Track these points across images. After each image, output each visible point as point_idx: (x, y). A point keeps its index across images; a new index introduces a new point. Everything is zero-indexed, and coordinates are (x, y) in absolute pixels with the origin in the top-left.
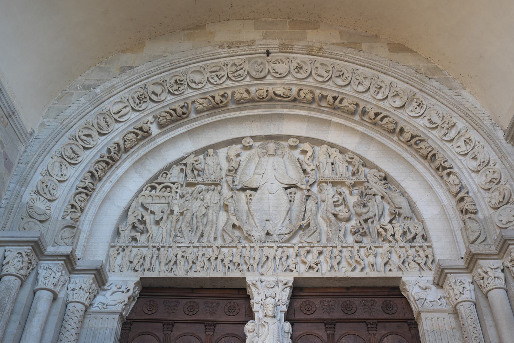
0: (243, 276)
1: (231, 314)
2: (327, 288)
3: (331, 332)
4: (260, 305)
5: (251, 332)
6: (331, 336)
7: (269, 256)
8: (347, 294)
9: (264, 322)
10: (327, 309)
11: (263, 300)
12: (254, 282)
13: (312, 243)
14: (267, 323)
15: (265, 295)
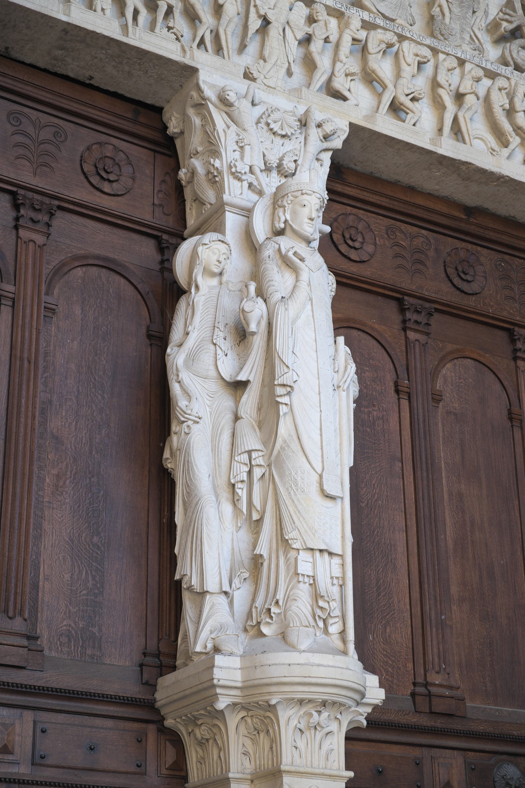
0: (187, 61)
1: (106, 187)
2: (412, 189)
3: (418, 336)
4: (245, 184)
5: (213, 275)
6: (417, 350)
7: (271, 17)
8: (463, 226)
9: (295, 254)
10: (403, 257)
11: (257, 170)
12: (232, 97)
13: (393, 20)
14: (302, 260)
15: (264, 156)
